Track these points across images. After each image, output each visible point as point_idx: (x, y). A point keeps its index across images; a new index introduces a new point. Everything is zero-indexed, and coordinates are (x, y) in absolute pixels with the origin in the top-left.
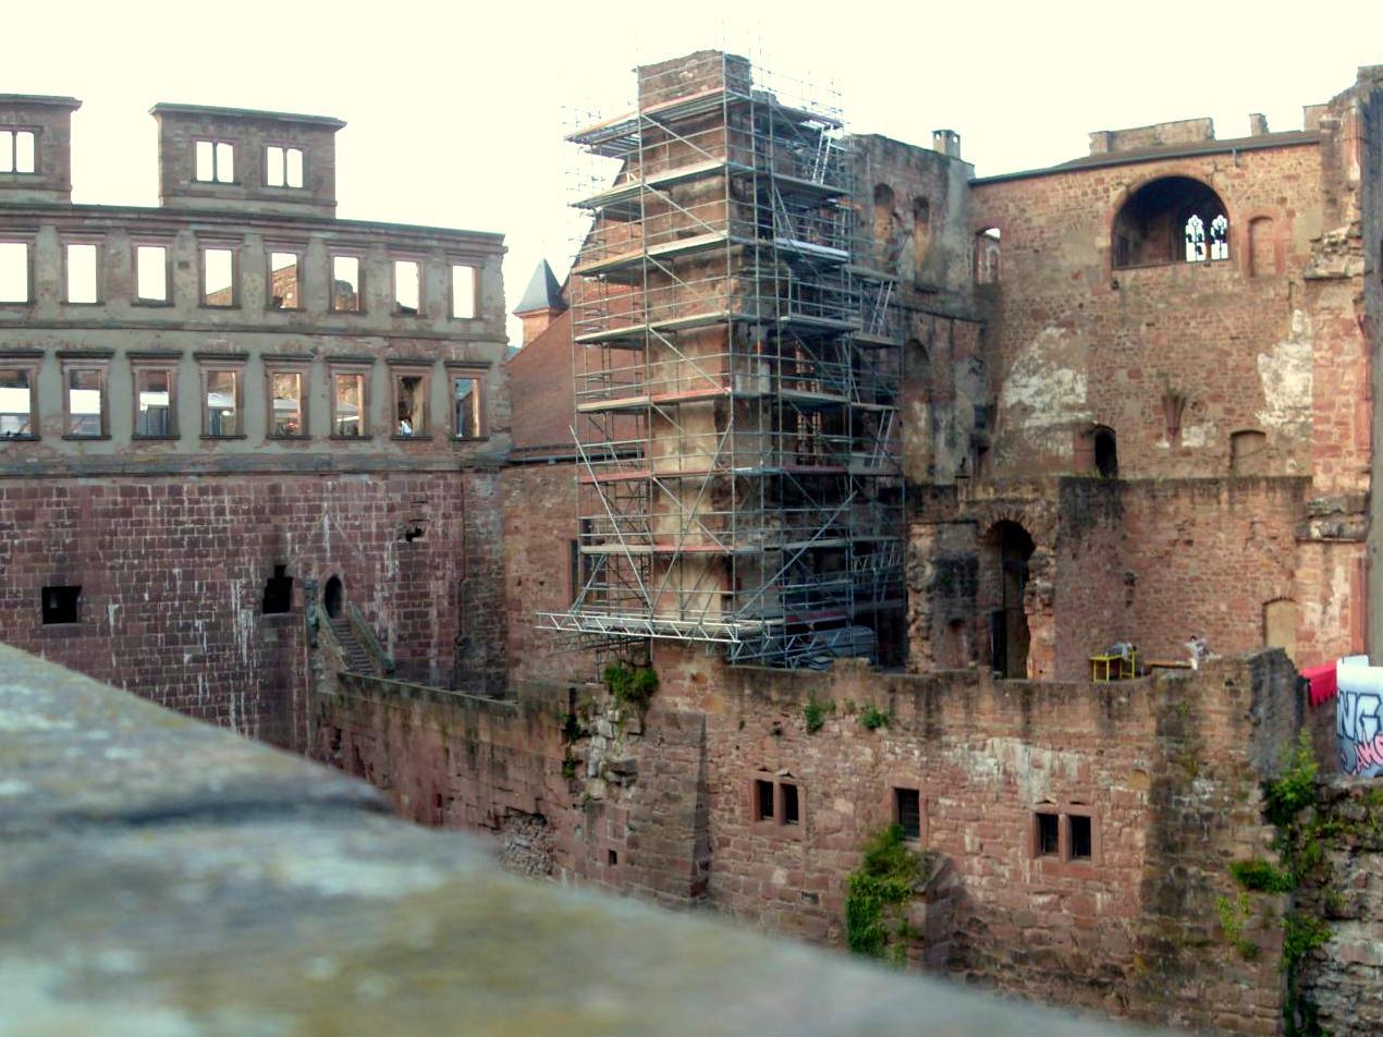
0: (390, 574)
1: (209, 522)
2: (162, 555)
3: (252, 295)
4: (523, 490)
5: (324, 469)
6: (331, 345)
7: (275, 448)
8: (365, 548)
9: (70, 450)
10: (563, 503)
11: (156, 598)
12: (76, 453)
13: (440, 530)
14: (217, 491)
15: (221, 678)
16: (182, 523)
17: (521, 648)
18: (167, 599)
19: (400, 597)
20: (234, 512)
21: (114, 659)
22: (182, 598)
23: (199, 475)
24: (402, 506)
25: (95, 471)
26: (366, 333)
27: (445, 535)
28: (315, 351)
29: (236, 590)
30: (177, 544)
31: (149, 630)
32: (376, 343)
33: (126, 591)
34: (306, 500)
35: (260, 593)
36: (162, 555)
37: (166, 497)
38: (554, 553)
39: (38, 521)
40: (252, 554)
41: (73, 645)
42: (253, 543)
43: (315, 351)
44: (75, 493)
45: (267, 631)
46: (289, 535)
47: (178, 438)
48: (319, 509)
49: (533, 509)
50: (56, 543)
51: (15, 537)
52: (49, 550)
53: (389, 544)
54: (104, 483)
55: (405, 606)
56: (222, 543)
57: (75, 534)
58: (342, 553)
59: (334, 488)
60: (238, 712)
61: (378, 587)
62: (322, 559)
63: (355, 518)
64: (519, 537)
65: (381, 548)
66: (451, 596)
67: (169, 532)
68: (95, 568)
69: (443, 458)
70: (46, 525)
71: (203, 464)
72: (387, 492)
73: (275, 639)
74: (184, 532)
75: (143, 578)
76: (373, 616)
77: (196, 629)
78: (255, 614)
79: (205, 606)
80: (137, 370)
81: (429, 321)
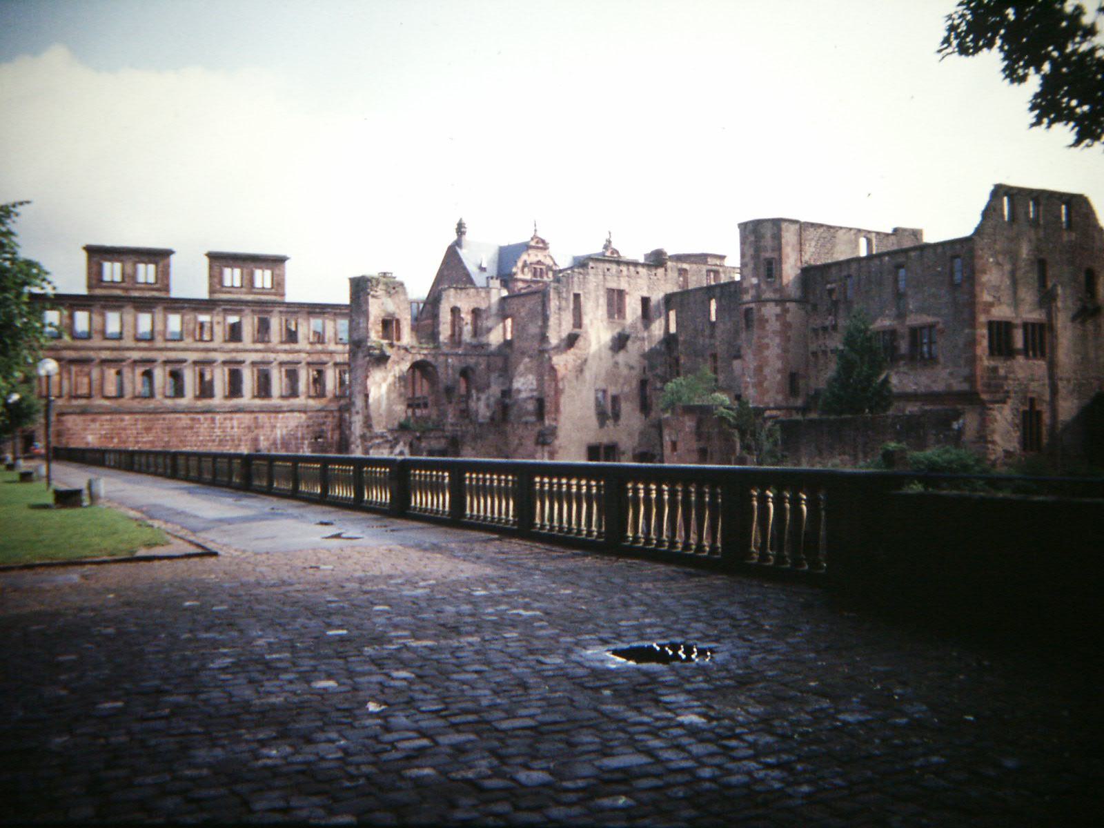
5: (277, 411)
6: (283, 357)
7: (258, 402)
14: (231, 419)
20: (239, 428)
26: (298, 351)
30: (214, 441)
32: (303, 355)
42: (246, 441)
44: (169, 419)
53: (306, 442)
54: (182, 416)
65: (303, 444)
67: (211, 436)
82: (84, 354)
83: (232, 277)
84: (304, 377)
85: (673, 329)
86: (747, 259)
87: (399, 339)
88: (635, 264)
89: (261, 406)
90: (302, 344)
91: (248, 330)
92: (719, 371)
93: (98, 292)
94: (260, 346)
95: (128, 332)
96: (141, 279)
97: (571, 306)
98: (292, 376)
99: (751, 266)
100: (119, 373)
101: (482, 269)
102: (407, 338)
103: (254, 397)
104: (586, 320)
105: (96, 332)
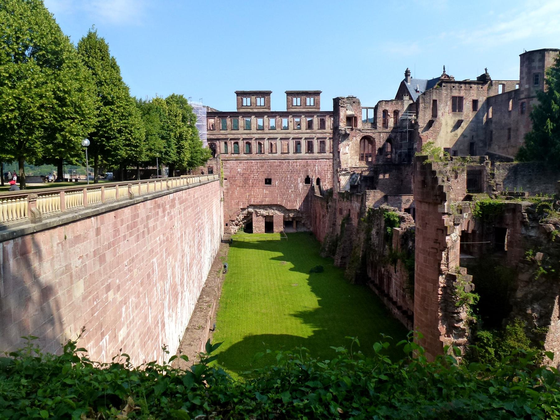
9: (270, 155)
14: (296, 162)
29: (299, 180)
30: (289, 171)
35: (304, 180)
58: (320, 173)
75: (282, 177)
76: (325, 185)
83: (297, 101)
85: (490, 116)
86: (524, 75)
87: (356, 126)
88: (470, 83)
91: (304, 125)
92: (512, 136)
93: (241, 110)
94: (308, 131)
96: (258, 104)
97: (431, 106)
98: (323, 143)
99: (525, 79)
100: (226, 143)
101: (417, 91)
102: (360, 125)
104: (439, 113)
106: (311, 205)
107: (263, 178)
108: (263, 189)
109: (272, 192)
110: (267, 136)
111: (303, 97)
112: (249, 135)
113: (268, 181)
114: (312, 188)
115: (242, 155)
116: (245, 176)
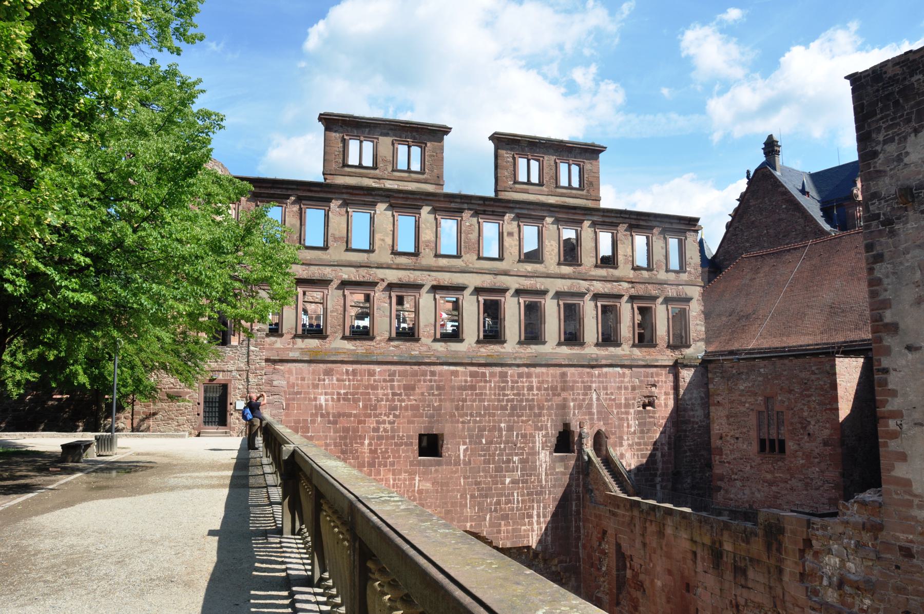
0: (632, 430)
1: (524, 395)
2: (494, 415)
3: (551, 254)
4: (723, 377)
6: (599, 287)
7: (565, 350)
8: (618, 413)
9: (440, 347)
10: (752, 386)
11: (490, 443)
12: (442, 349)
13: (663, 402)
14: (529, 375)
15: (528, 494)
16: (507, 395)
17: (722, 480)
18: (497, 443)
19: (639, 444)
20: (539, 389)
21: (462, 481)
22: (507, 442)
23: (518, 366)
24: (640, 387)
25: (454, 361)
27: (666, 405)
28: (588, 290)
29: (539, 438)
30: (504, 408)
31: (485, 462)
32: (625, 285)
33: (471, 437)
34: (583, 382)
35: (554, 440)
36: (494, 415)
37: (497, 379)
38: (746, 419)
39: (417, 391)
40: (550, 415)
41: (436, 471)
42: (549, 408)
43: (588, 290)
44: (441, 374)
45: (557, 464)
46: (572, 404)
47: (505, 342)
48: (590, 388)
49: (730, 390)
50: (429, 406)
51: (403, 401)
52: (424, 410)
54: (460, 369)
55: (641, 450)
56: (531, 408)
57: (440, 400)
58: (604, 415)
59: (599, 375)
60: (539, 516)
61: (625, 438)
62: (592, 419)
63: (612, 394)
64: (721, 408)
65: (627, 413)
66: (669, 444)
67: (499, 401)
68: (452, 422)
69: (665, 357)
70: (422, 394)
71: (521, 358)
72: (631, 377)
73: (562, 470)
74: (508, 401)
75: (482, 430)
77: (514, 462)
78: (551, 453)
79: (520, 448)
80: (481, 299)
81: (655, 272)
82: (315, 272)
83: (527, 169)
84: (627, 315)
89: (569, 357)
90: (623, 270)
91: (552, 251)
93: (340, 180)
94: (567, 270)
95: (383, 239)
98: (609, 313)
103: (560, 344)
105: (336, 239)
106: (578, 529)
107: (411, 430)
108: (412, 474)
109: (442, 485)
110: (429, 279)
111: (549, 160)
112: (363, 271)
113: (430, 445)
114: (584, 469)
115: (337, 344)
116: (343, 422)
